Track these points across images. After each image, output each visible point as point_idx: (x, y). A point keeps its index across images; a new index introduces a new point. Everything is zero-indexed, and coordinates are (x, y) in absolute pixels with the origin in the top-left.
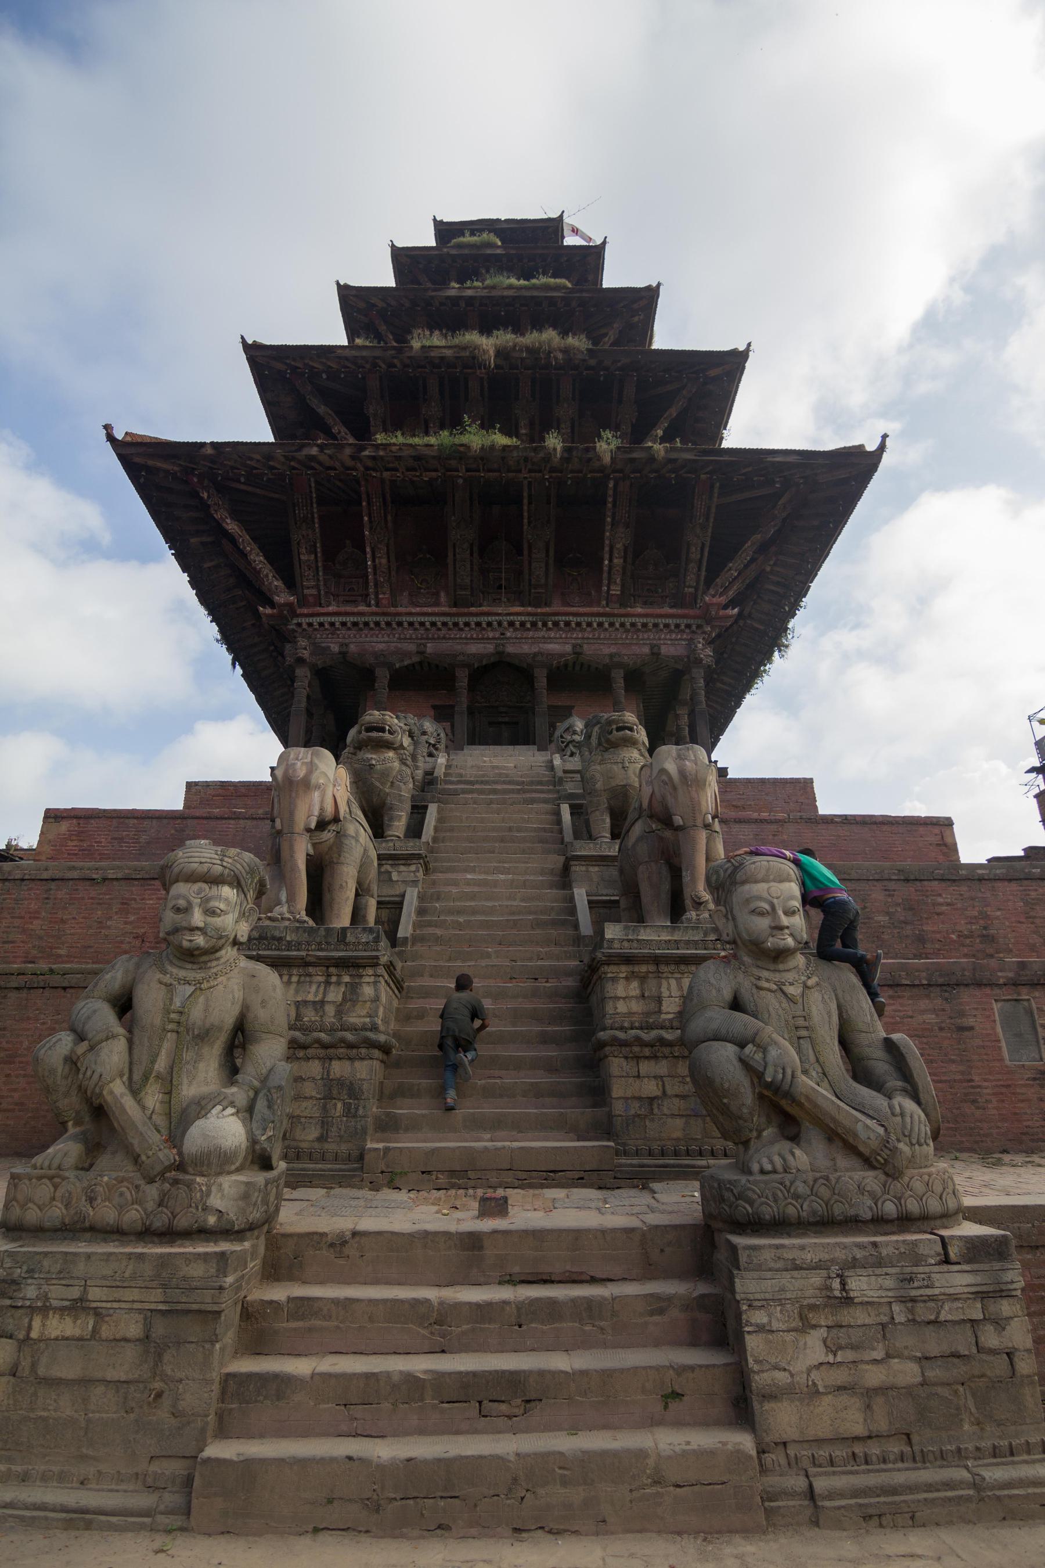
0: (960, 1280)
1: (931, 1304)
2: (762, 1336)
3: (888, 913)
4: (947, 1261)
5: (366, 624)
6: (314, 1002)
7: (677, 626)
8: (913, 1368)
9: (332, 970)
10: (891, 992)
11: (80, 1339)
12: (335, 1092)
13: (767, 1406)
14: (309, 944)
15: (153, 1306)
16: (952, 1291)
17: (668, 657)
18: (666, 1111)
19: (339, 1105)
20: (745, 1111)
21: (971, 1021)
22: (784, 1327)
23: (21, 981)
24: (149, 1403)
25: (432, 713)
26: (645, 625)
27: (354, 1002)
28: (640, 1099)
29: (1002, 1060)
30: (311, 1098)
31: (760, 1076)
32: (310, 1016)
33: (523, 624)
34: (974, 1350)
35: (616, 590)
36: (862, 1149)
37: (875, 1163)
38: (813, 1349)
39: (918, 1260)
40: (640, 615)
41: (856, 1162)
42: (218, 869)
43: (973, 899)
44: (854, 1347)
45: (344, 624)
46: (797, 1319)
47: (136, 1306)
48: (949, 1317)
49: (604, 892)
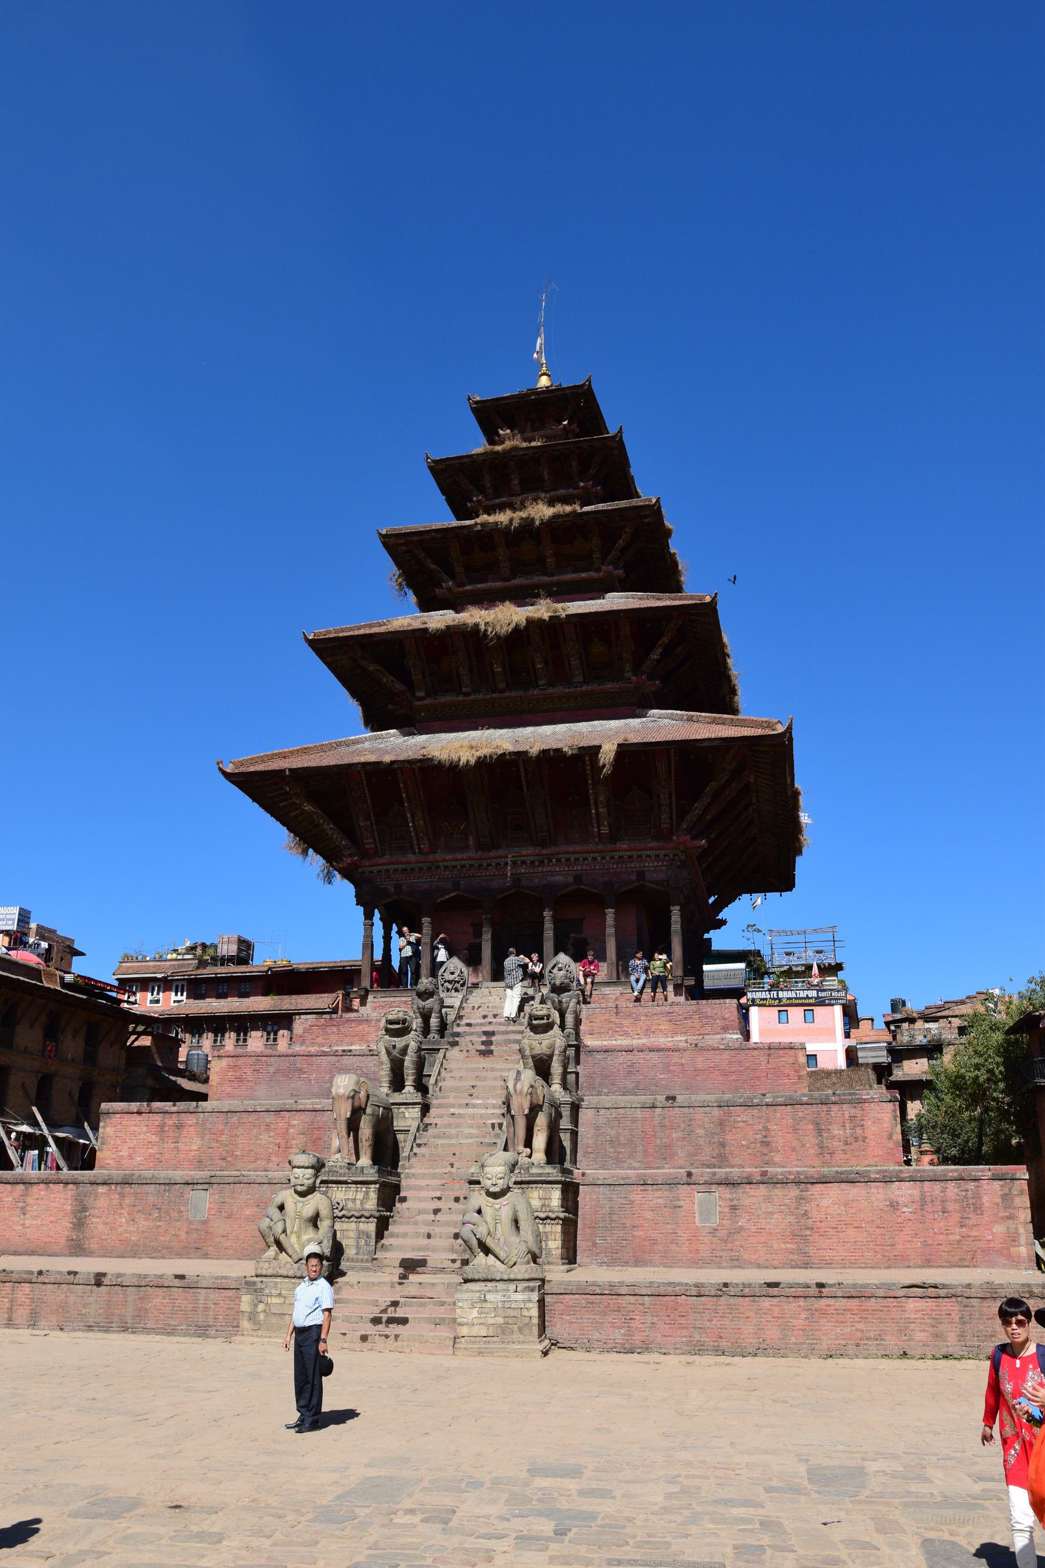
0: (519, 1296)
5: (413, 869)
7: (657, 856)
10: (642, 1188)
17: (651, 882)
21: (682, 1203)
23: (231, 1180)
26: (630, 857)
27: (368, 1199)
33: (532, 862)
35: (605, 830)
38: (475, 1313)
39: (507, 1290)
40: (625, 850)
42: (307, 1164)
45: (396, 870)
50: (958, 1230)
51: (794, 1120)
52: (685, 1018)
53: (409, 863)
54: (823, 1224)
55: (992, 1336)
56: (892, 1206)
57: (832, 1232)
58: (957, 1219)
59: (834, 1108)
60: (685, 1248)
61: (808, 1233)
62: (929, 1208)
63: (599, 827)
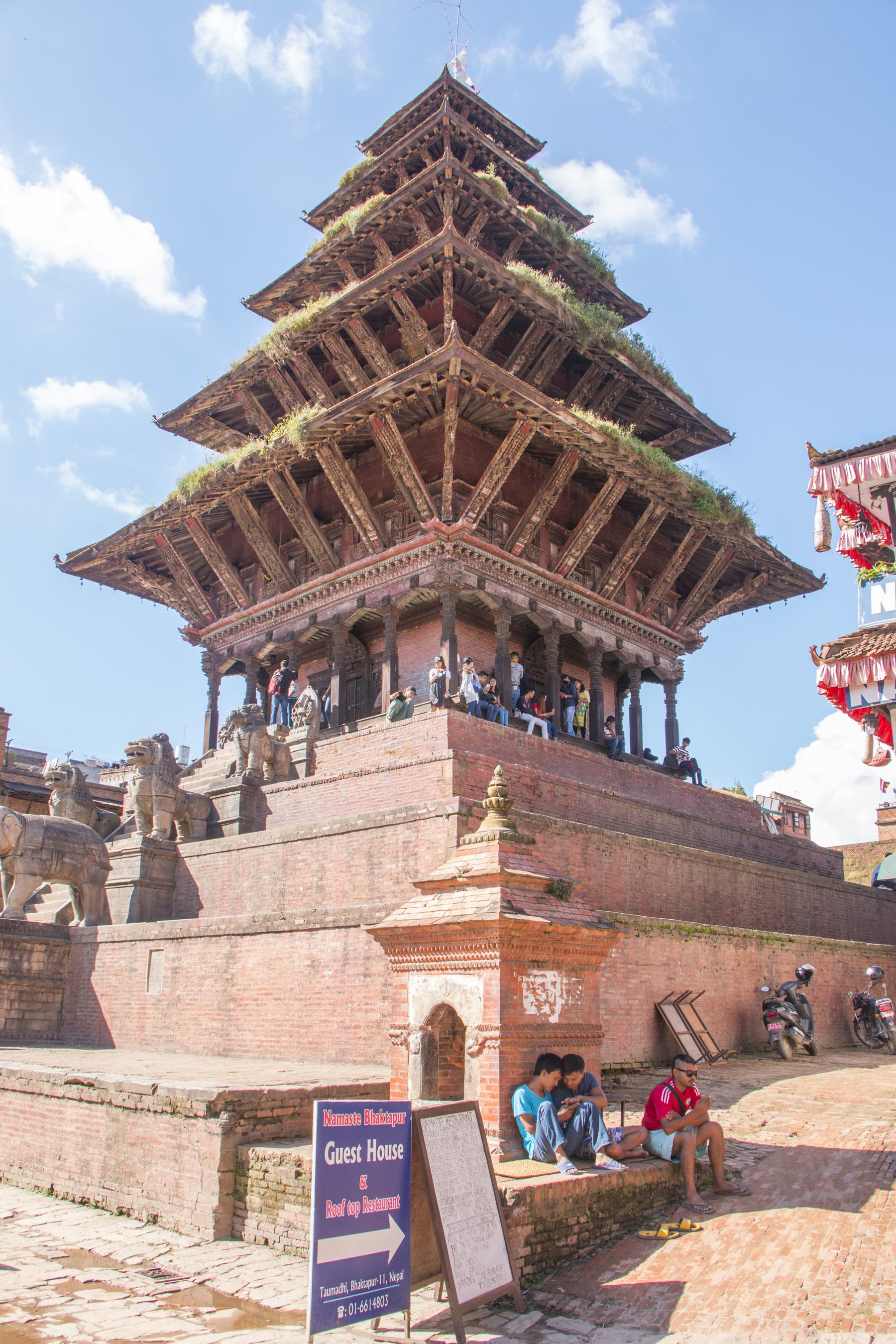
7: (424, 552)
10: (111, 946)
17: (423, 587)
26: (401, 561)
43: (318, 853)
50: (379, 1004)
51: (349, 854)
52: (399, 743)
53: (232, 621)
54: (246, 994)
55: (131, 1174)
56: (313, 967)
57: (253, 1005)
58: (379, 987)
59: (389, 831)
61: (232, 1006)
62: (351, 970)
63: (366, 535)
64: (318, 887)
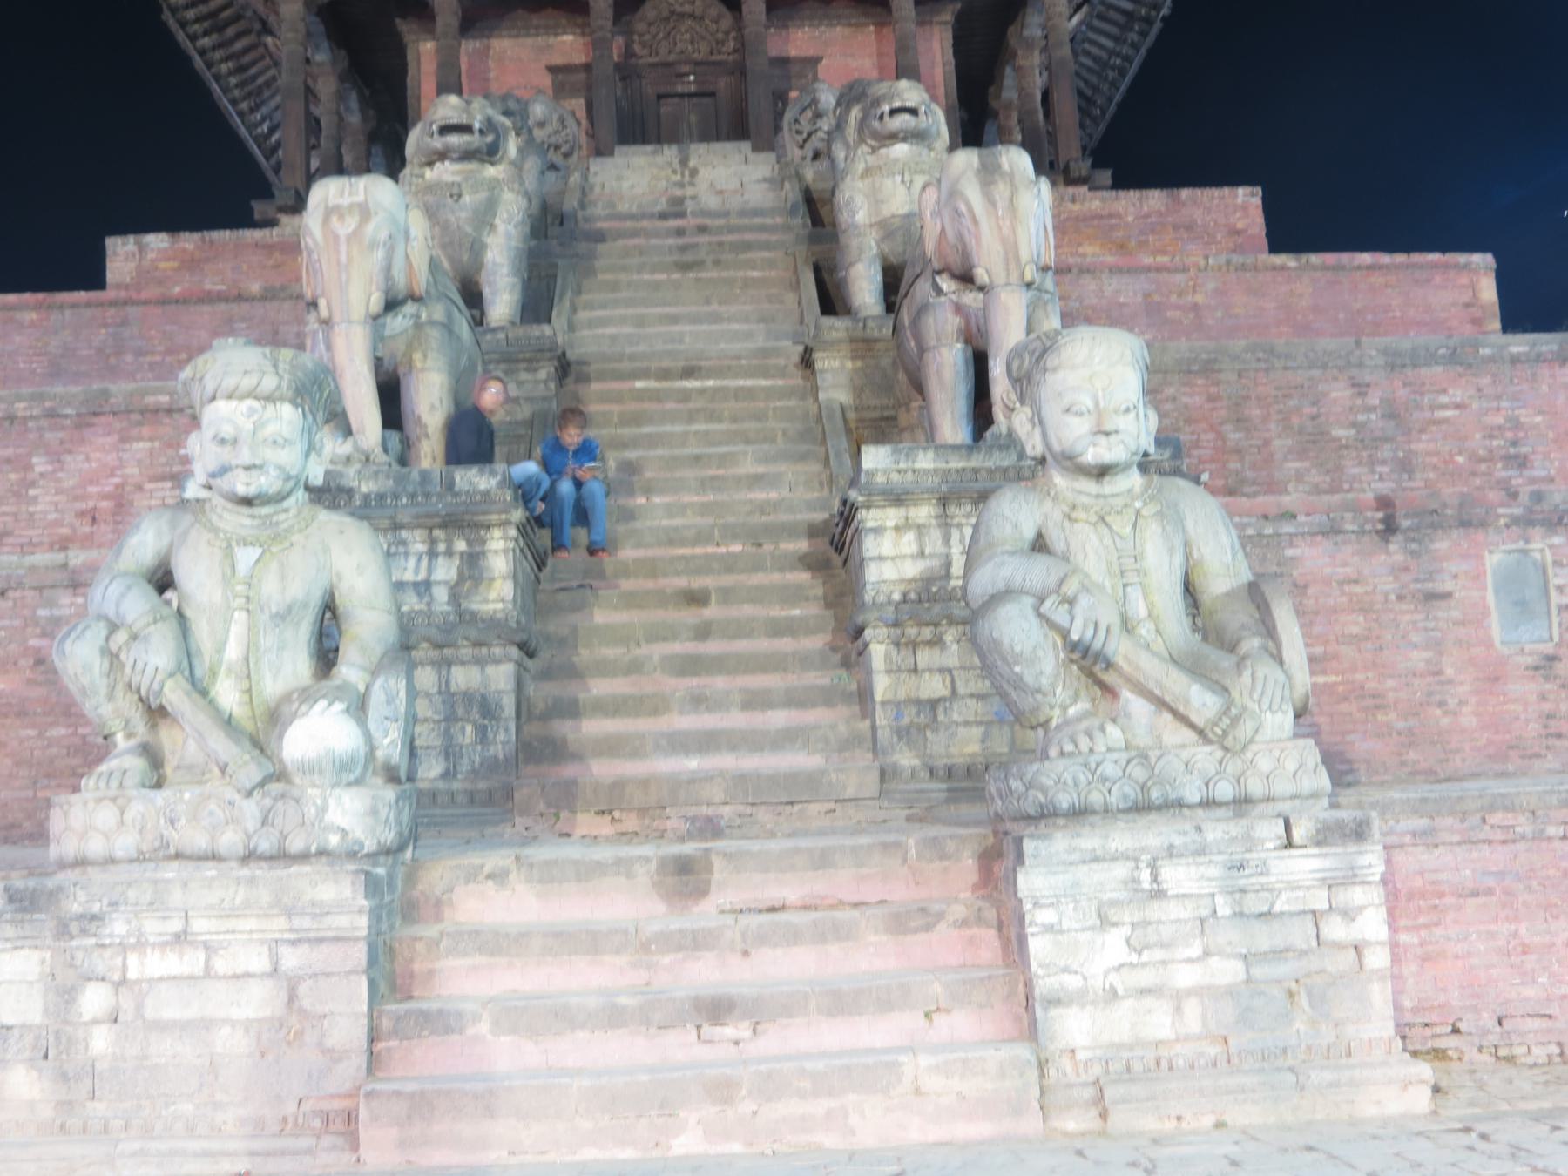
1: (1266, 894)
2: (1048, 937)
3: (1354, 425)
4: (1289, 844)
6: (416, 585)
8: (1239, 966)
9: (437, 533)
11: (191, 977)
12: (460, 712)
13: (1053, 1012)
14: (396, 496)
15: (278, 936)
16: (1291, 878)
18: (956, 717)
19: (469, 729)
20: (1044, 681)
21: (1449, 586)
22: (1076, 926)
24: (289, 1043)
25: (547, 81)
28: (918, 702)
29: (1489, 645)
30: (426, 720)
31: (1065, 634)
32: (412, 602)
34: (1314, 943)
36: (1194, 718)
37: (1211, 735)
39: (1250, 843)
41: (1189, 735)
44: (1164, 946)
46: (1094, 915)
47: (255, 936)
48: (1286, 908)
49: (873, 402)
60: (1468, 719)
64: (1508, 459)
